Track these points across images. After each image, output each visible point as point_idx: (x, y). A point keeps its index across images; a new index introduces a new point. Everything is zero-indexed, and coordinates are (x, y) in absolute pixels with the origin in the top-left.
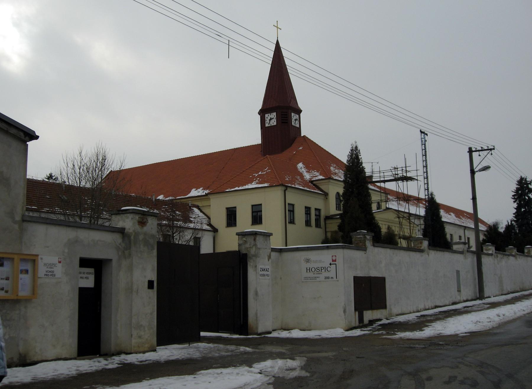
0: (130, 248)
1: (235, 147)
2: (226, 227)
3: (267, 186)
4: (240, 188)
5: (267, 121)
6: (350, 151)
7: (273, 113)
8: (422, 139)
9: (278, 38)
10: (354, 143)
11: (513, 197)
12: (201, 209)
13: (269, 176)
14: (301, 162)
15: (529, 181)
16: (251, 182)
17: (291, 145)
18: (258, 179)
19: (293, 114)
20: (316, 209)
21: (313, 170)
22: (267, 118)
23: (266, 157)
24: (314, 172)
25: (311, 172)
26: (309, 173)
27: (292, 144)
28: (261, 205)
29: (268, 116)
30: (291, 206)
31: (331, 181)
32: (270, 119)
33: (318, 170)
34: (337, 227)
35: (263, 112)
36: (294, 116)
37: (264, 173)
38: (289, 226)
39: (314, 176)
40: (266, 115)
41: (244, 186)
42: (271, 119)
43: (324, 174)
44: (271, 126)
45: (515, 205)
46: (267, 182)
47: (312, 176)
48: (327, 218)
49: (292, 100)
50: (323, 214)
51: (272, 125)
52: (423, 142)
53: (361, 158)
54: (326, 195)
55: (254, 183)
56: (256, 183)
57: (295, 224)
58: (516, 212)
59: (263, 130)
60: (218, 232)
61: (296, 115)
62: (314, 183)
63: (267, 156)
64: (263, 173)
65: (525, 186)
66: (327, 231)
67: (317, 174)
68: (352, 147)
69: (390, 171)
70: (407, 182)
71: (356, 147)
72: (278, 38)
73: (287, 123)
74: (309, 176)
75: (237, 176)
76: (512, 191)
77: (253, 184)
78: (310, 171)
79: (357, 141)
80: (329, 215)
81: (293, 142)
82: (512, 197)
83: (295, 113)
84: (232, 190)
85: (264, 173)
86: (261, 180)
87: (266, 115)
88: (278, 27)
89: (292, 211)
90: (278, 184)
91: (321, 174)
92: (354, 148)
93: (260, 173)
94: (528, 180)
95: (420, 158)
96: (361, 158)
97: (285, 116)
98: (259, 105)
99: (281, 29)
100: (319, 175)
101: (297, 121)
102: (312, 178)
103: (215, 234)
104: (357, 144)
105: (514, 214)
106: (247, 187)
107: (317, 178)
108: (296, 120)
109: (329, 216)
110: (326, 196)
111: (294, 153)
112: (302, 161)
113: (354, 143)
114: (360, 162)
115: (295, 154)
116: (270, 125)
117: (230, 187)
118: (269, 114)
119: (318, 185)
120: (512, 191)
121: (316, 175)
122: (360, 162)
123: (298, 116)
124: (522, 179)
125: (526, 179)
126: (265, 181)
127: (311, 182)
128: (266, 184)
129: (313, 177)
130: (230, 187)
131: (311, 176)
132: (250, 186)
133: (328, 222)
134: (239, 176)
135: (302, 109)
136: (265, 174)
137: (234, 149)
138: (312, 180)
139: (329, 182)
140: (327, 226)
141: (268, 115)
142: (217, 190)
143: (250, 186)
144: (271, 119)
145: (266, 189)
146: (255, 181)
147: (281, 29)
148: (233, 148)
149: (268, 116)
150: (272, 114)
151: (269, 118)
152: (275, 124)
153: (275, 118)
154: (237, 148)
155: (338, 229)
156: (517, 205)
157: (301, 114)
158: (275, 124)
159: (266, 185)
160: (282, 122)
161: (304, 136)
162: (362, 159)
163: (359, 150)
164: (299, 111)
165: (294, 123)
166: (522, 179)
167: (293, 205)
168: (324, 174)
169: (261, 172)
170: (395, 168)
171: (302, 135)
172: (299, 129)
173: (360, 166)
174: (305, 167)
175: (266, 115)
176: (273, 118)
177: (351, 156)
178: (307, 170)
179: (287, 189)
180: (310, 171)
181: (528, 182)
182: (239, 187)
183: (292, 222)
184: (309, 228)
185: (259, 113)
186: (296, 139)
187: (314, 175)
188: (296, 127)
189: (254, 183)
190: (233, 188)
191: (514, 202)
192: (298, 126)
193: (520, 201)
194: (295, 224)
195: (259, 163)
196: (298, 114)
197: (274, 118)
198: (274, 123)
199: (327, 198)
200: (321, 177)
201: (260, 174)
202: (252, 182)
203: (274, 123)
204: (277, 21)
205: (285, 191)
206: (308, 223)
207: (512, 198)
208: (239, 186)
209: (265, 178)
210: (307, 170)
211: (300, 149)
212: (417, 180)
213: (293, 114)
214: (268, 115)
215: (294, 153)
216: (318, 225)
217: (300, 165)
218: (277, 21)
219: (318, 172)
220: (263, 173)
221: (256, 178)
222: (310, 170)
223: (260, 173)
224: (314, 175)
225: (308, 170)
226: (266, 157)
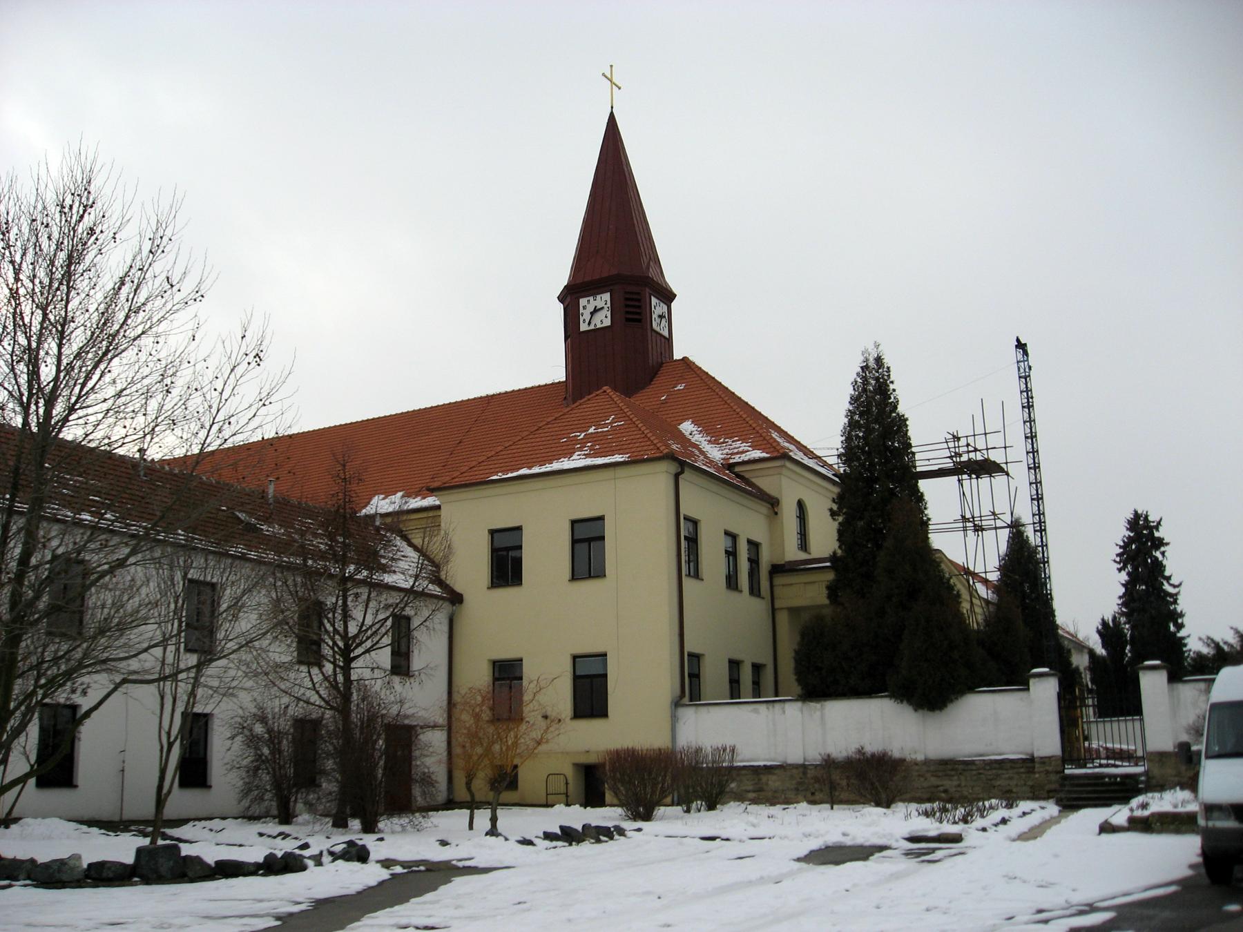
0: (138, 313)
1: (491, 392)
2: (488, 588)
3: (622, 460)
4: (536, 470)
5: (585, 315)
6: (859, 370)
7: (602, 295)
8: (1018, 362)
9: (612, 108)
10: (871, 348)
11: (1118, 559)
12: (410, 537)
13: (624, 437)
14: (688, 419)
15: (1153, 522)
16: (569, 454)
17: (652, 380)
18: (589, 444)
19: (654, 301)
20: (750, 542)
21: (730, 438)
22: (584, 308)
23: (602, 391)
24: (733, 442)
25: (723, 443)
26: (718, 444)
27: (654, 377)
28: (601, 518)
29: (586, 303)
30: (690, 525)
31: (788, 464)
32: (592, 310)
33: (743, 437)
34: (825, 592)
35: (571, 296)
36: (658, 307)
37: (606, 429)
38: (688, 583)
39: (736, 451)
40: (581, 300)
41: (547, 465)
42: (596, 310)
43: (763, 446)
44: (596, 330)
45: (1123, 577)
46: (621, 452)
47: (730, 452)
48: (777, 569)
49: (651, 263)
50: (766, 558)
51: (599, 326)
52: (1022, 370)
53: (894, 390)
54: (773, 503)
55: (579, 455)
56: (584, 455)
57: (703, 580)
58: (1124, 594)
59: (572, 341)
60: (464, 602)
61: (662, 304)
62: (737, 469)
63: (605, 388)
64: (600, 430)
65: (1145, 532)
66: (777, 606)
67: (744, 446)
68: (866, 360)
69: (945, 445)
70: (977, 478)
71: (879, 360)
72: (612, 108)
73: (639, 321)
74: (720, 452)
75: (521, 442)
76: (1117, 545)
77: (575, 457)
78: (722, 440)
79: (879, 341)
80: (783, 563)
81: (656, 374)
82: (1114, 557)
83: (658, 299)
84: (510, 475)
85: (606, 429)
86: (597, 447)
87: (583, 302)
88: (614, 80)
89: (693, 541)
90: (655, 455)
91: (754, 447)
92: (872, 363)
93: (592, 430)
94: (1150, 519)
95: (1016, 414)
96: (894, 390)
97: (637, 304)
98: (561, 276)
99: (619, 88)
100: (750, 449)
101: (663, 320)
102: (730, 458)
103: (454, 608)
104: (880, 349)
105: (1120, 598)
106: (556, 466)
107: (745, 457)
108: (661, 317)
109: (783, 566)
110: (773, 505)
111: (663, 398)
112: (691, 416)
113: (871, 348)
114: (890, 401)
115: (665, 402)
116: (592, 327)
117: (502, 469)
118: (591, 299)
119: (747, 475)
120: (1117, 545)
121: (741, 449)
122: (890, 401)
123: (665, 308)
124: (1137, 515)
125: (1147, 516)
126: (613, 448)
127: (726, 466)
128: (616, 456)
129: (732, 454)
130: (502, 469)
131: (725, 452)
132: (566, 464)
133: (780, 580)
134: (527, 441)
135: (675, 290)
136: (608, 431)
137: (487, 396)
138: (731, 461)
139: (782, 466)
140: (777, 591)
141: (588, 301)
142: (462, 479)
143: (566, 464)
144: (596, 310)
145: (621, 472)
146: (581, 449)
147: (619, 88)
148: (484, 394)
149: (587, 304)
150: (598, 297)
151: (591, 308)
152: (607, 322)
153: (606, 309)
154: (494, 395)
155: (829, 597)
156: (1126, 578)
157: (673, 304)
158: (607, 322)
159: (618, 458)
160: (628, 320)
161: (685, 360)
162: (897, 392)
163: (888, 368)
164: (668, 296)
165: (659, 326)
166: (1137, 515)
167: (695, 523)
168: (763, 446)
169: (593, 428)
170: (954, 437)
171: (677, 355)
172: (669, 341)
173: (892, 412)
174: (701, 431)
175: (583, 302)
176: (602, 308)
177: (865, 380)
178: (709, 438)
179: (682, 472)
180: (722, 440)
181: (1152, 524)
182: (530, 468)
183: (696, 575)
184: (733, 595)
185: (561, 298)
186: (661, 367)
187: (735, 448)
188: (661, 335)
189: (579, 455)
190: (512, 471)
191: (1120, 570)
192: (666, 333)
193: (1135, 568)
194: (703, 580)
195: (582, 407)
196: (665, 304)
197: (606, 306)
198: (604, 320)
199: (776, 513)
200: (757, 454)
201: (592, 433)
202: (571, 454)
203: (604, 320)
204: (611, 66)
205: (677, 477)
206: (732, 582)
207: (1115, 561)
208: (530, 465)
209: (609, 441)
210: (709, 438)
211: (679, 390)
212: (1008, 474)
213: (654, 301)
214: (588, 301)
215: (663, 398)
216: (755, 591)
217: (687, 427)
218: (611, 66)
219: (744, 441)
220: (600, 430)
221: (583, 443)
222: (719, 437)
223: (592, 430)
224: (735, 448)
225: (712, 437)
226: (602, 391)
